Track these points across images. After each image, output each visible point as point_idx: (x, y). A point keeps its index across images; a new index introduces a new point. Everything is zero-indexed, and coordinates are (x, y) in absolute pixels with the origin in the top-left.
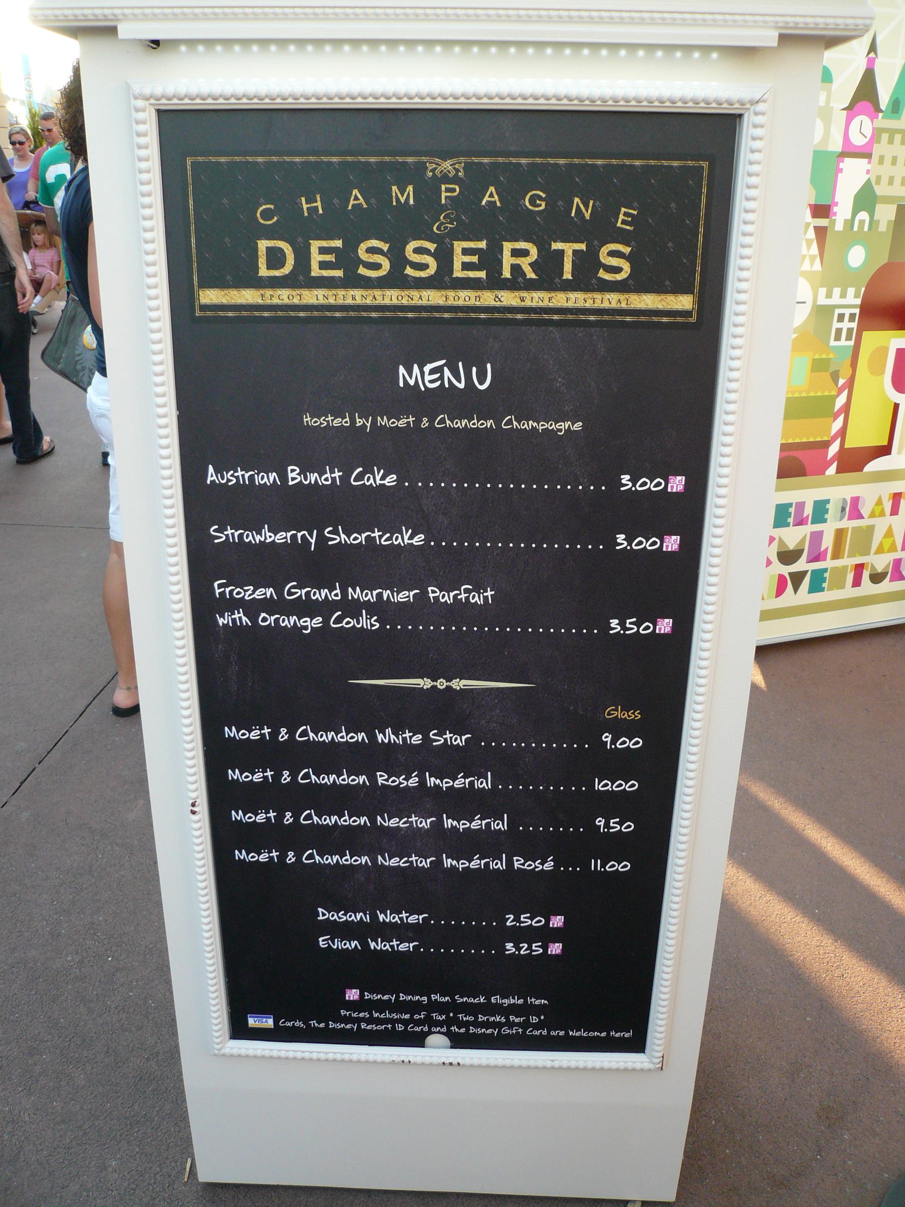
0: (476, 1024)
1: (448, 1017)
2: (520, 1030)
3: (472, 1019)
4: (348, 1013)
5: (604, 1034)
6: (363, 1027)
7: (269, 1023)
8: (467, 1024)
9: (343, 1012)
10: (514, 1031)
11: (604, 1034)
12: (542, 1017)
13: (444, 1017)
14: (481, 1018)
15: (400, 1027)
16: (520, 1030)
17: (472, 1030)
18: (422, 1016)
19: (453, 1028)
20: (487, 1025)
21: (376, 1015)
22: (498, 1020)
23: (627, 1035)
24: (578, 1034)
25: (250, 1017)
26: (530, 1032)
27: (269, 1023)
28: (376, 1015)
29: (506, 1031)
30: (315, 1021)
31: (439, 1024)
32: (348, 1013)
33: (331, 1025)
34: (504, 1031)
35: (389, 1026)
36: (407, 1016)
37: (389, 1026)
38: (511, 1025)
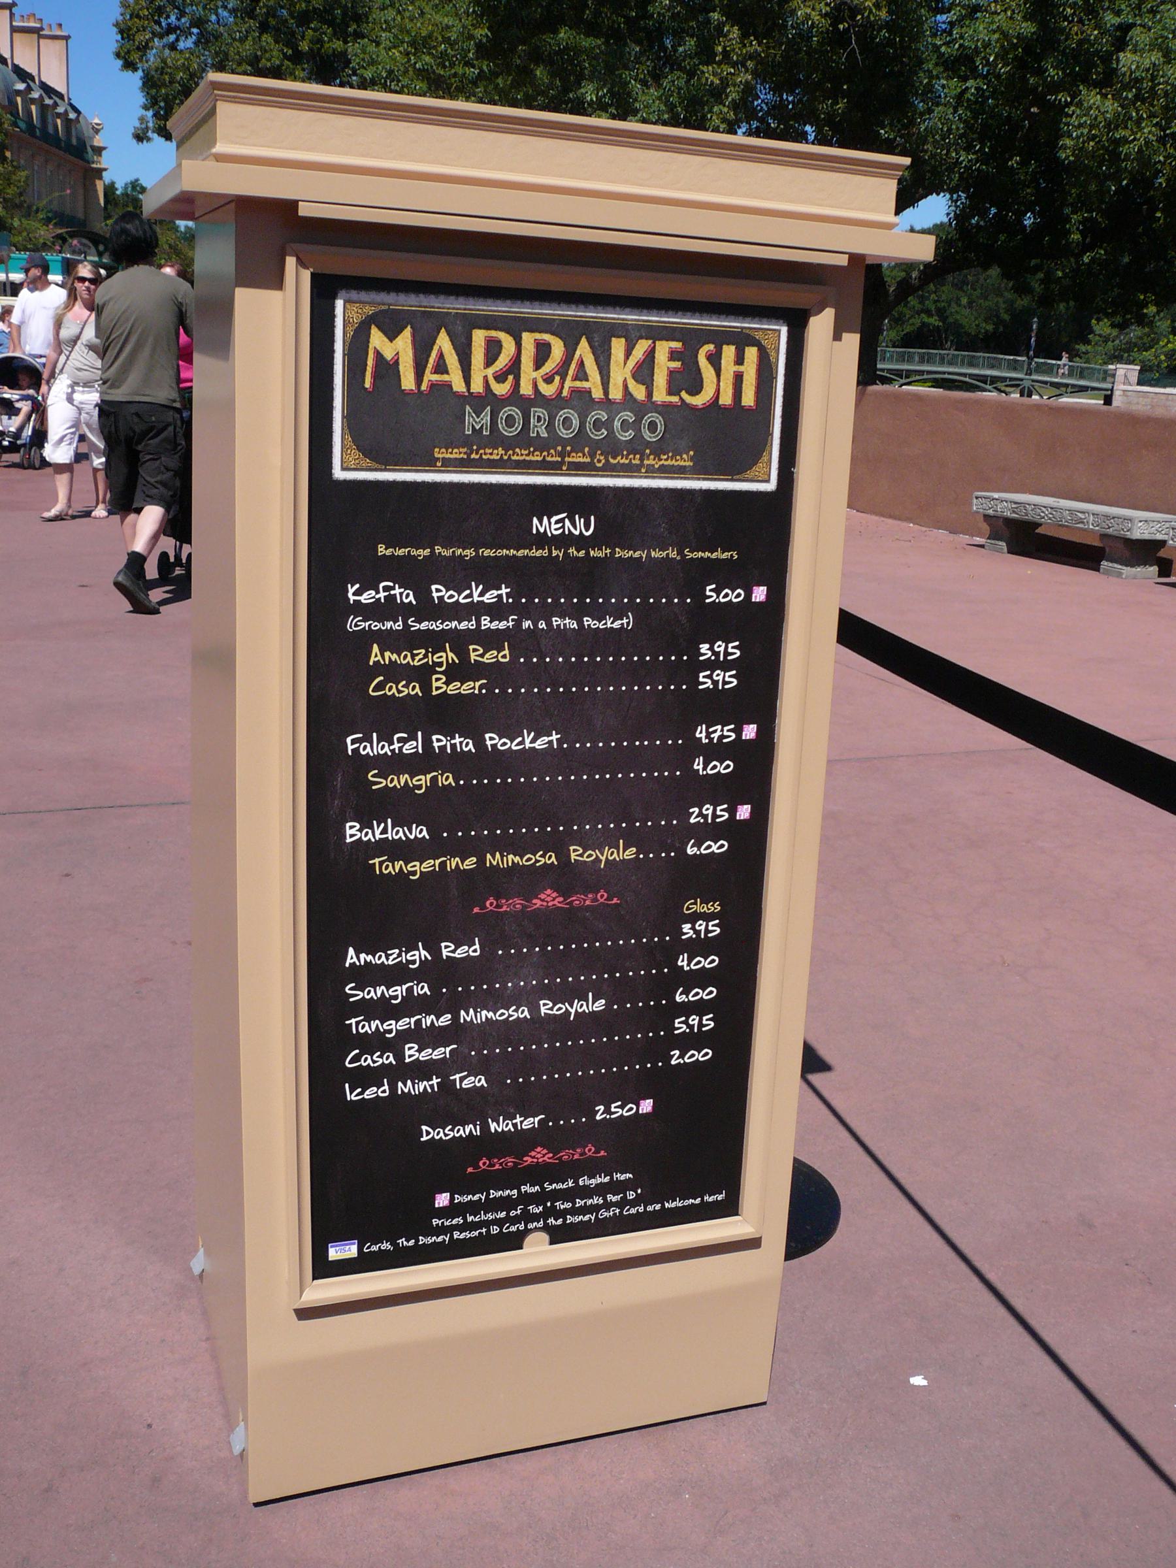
0: (574, 1211)
1: (545, 1207)
2: (618, 1211)
3: (568, 1205)
4: (440, 1222)
5: (698, 1201)
6: (455, 1237)
7: (350, 1250)
8: (563, 1214)
9: (435, 1222)
10: (611, 1213)
11: (698, 1201)
12: (639, 1191)
13: (541, 1208)
14: (579, 1203)
15: (495, 1230)
16: (618, 1211)
17: (570, 1219)
18: (519, 1212)
19: (549, 1221)
20: (584, 1210)
21: (470, 1219)
22: (596, 1202)
23: (720, 1197)
24: (673, 1205)
25: (331, 1247)
26: (628, 1210)
27: (350, 1250)
28: (470, 1219)
29: (604, 1214)
30: (404, 1239)
31: (535, 1218)
32: (440, 1222)
33: (422, 1240)
34: (601, 1215)
35: (484, 1230)
36: (503, 1215)
37: (484, 1230)
38: (607, 1205)
